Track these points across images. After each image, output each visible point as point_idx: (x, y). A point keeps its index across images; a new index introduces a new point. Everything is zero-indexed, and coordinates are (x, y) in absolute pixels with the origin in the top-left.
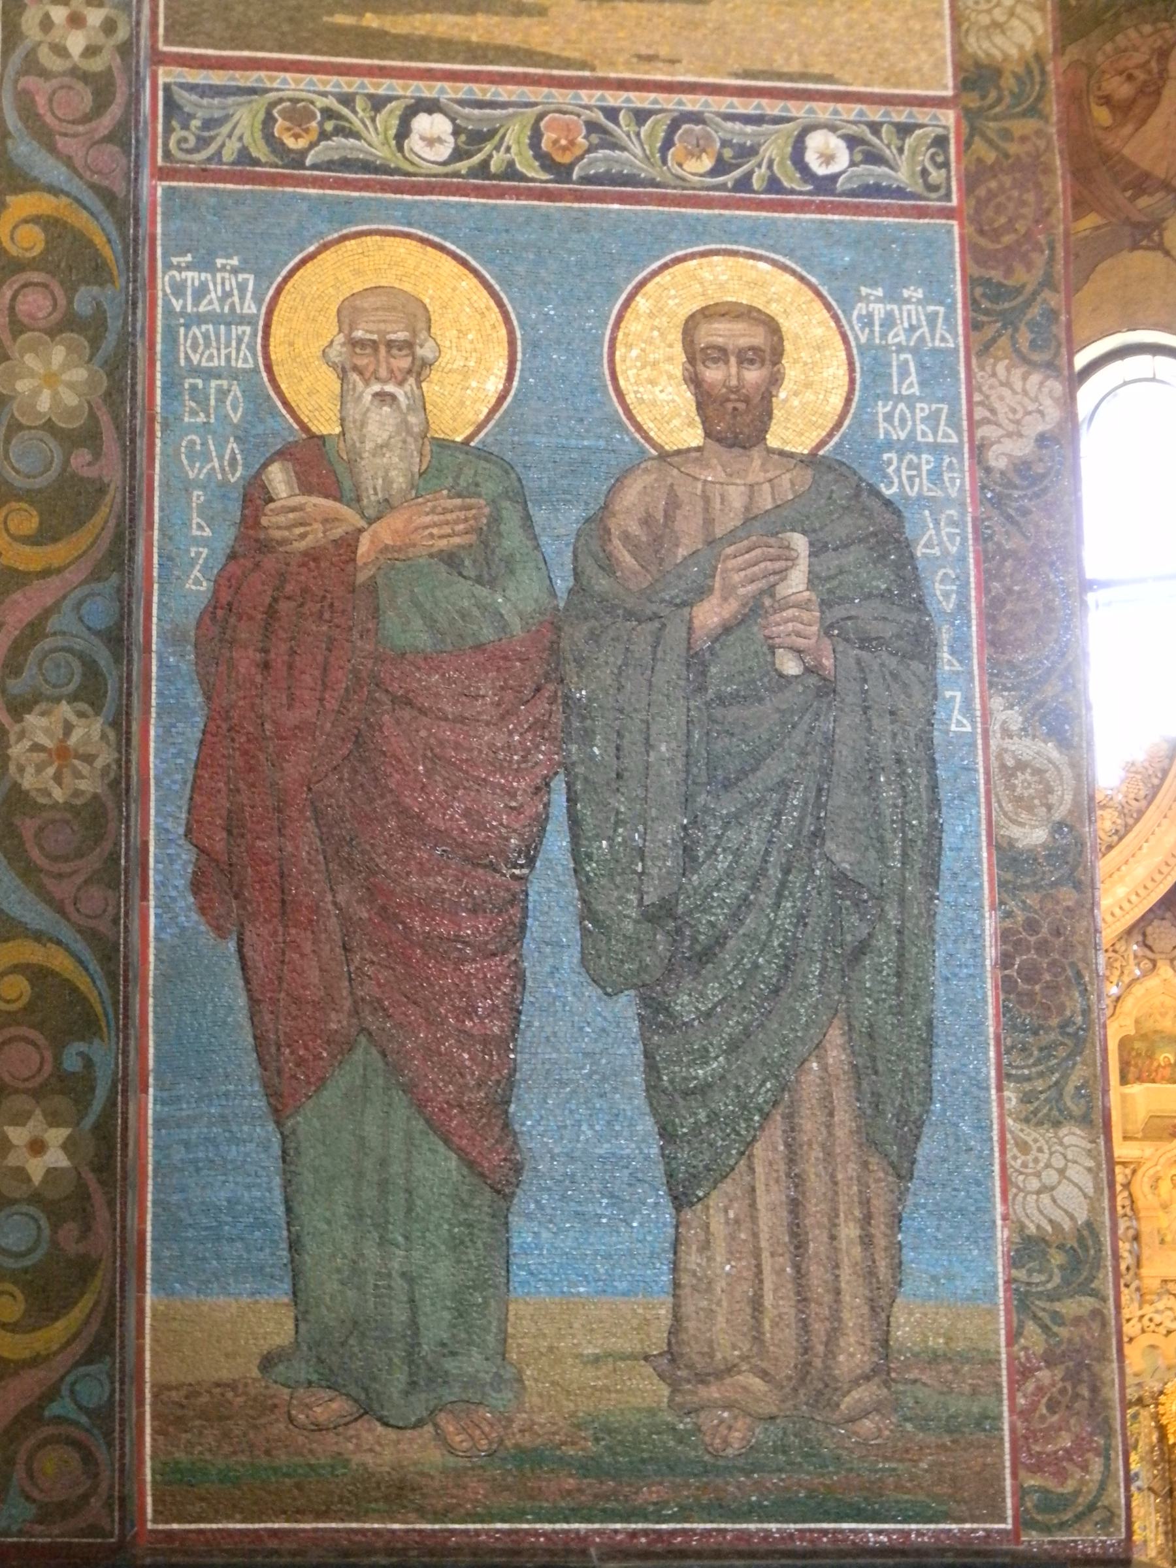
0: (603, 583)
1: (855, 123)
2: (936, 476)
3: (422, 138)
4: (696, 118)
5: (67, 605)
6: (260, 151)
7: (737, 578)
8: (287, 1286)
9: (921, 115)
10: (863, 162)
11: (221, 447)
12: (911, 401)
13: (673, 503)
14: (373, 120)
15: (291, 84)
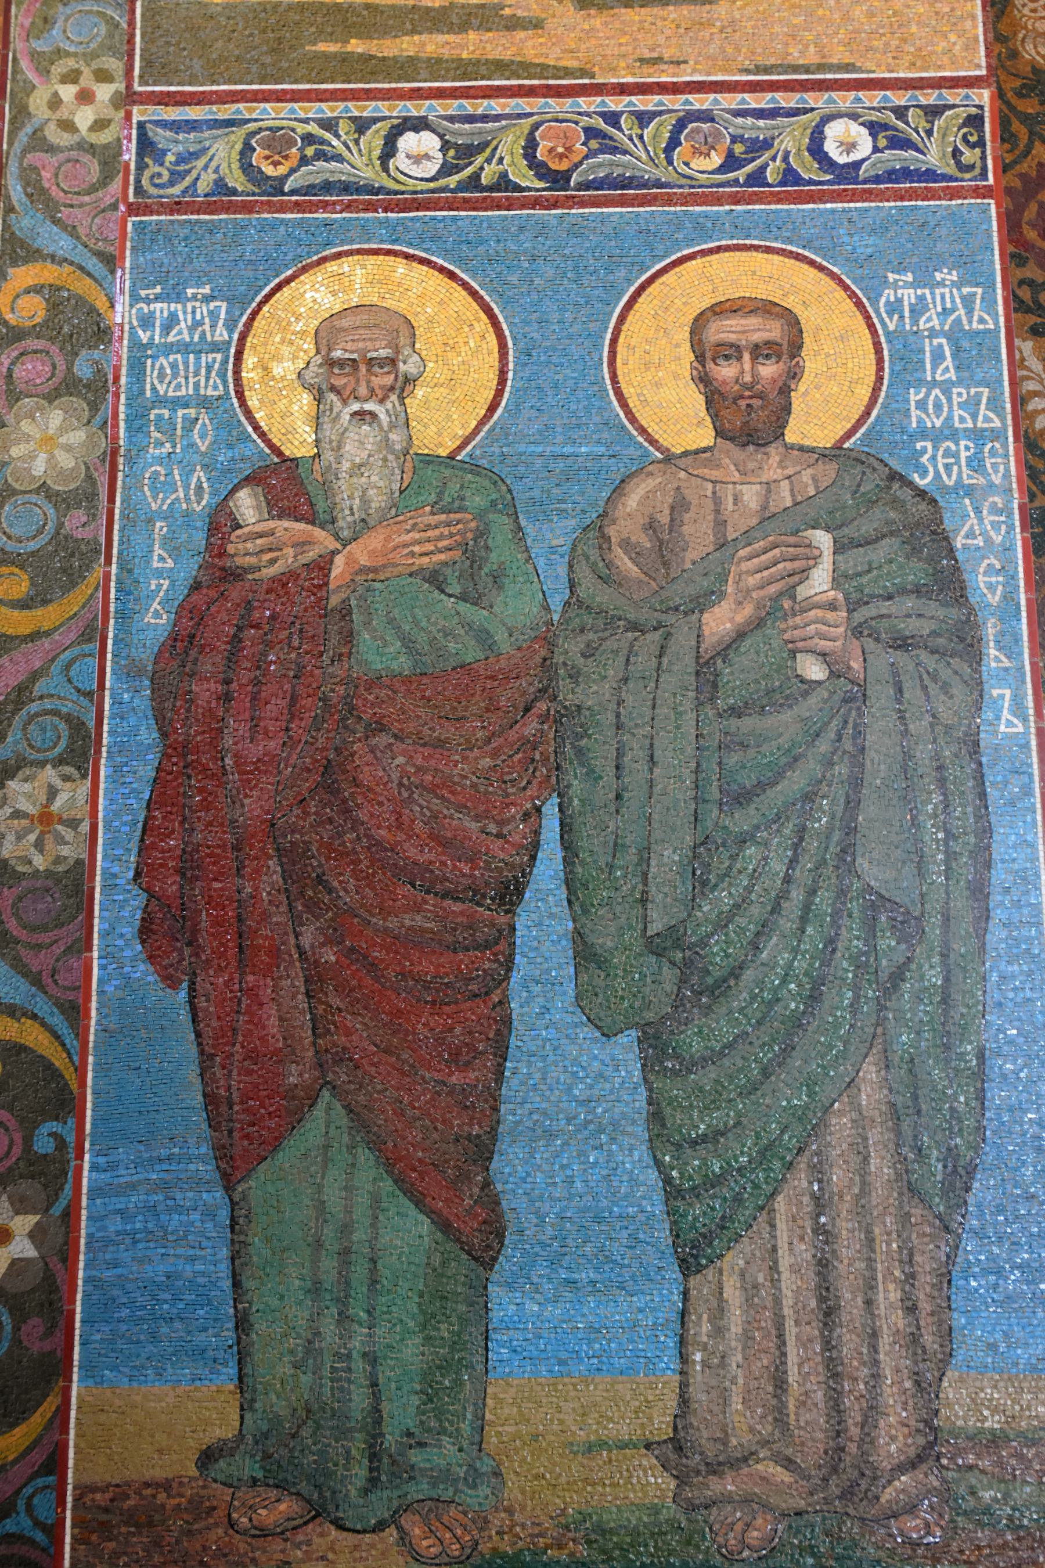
0: (603, 597)
1: (878, 110)
2: (977, 464)
3: (408, 157)
4: (706, 116)
5: (56, 668)
6: (236, 180)
7: (752, 581)
8: (232, 1370)
9: (951, 96)
10: (887, 148)
11: (187, 475)
12: (946, 388)
13: (679, 506)
14: (357, 142)
15: (270, 113)
